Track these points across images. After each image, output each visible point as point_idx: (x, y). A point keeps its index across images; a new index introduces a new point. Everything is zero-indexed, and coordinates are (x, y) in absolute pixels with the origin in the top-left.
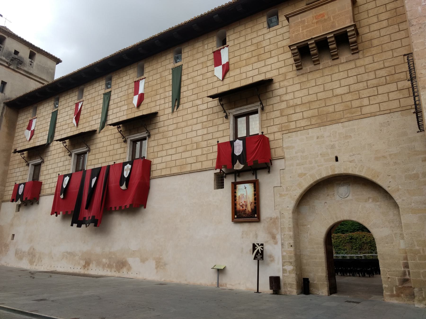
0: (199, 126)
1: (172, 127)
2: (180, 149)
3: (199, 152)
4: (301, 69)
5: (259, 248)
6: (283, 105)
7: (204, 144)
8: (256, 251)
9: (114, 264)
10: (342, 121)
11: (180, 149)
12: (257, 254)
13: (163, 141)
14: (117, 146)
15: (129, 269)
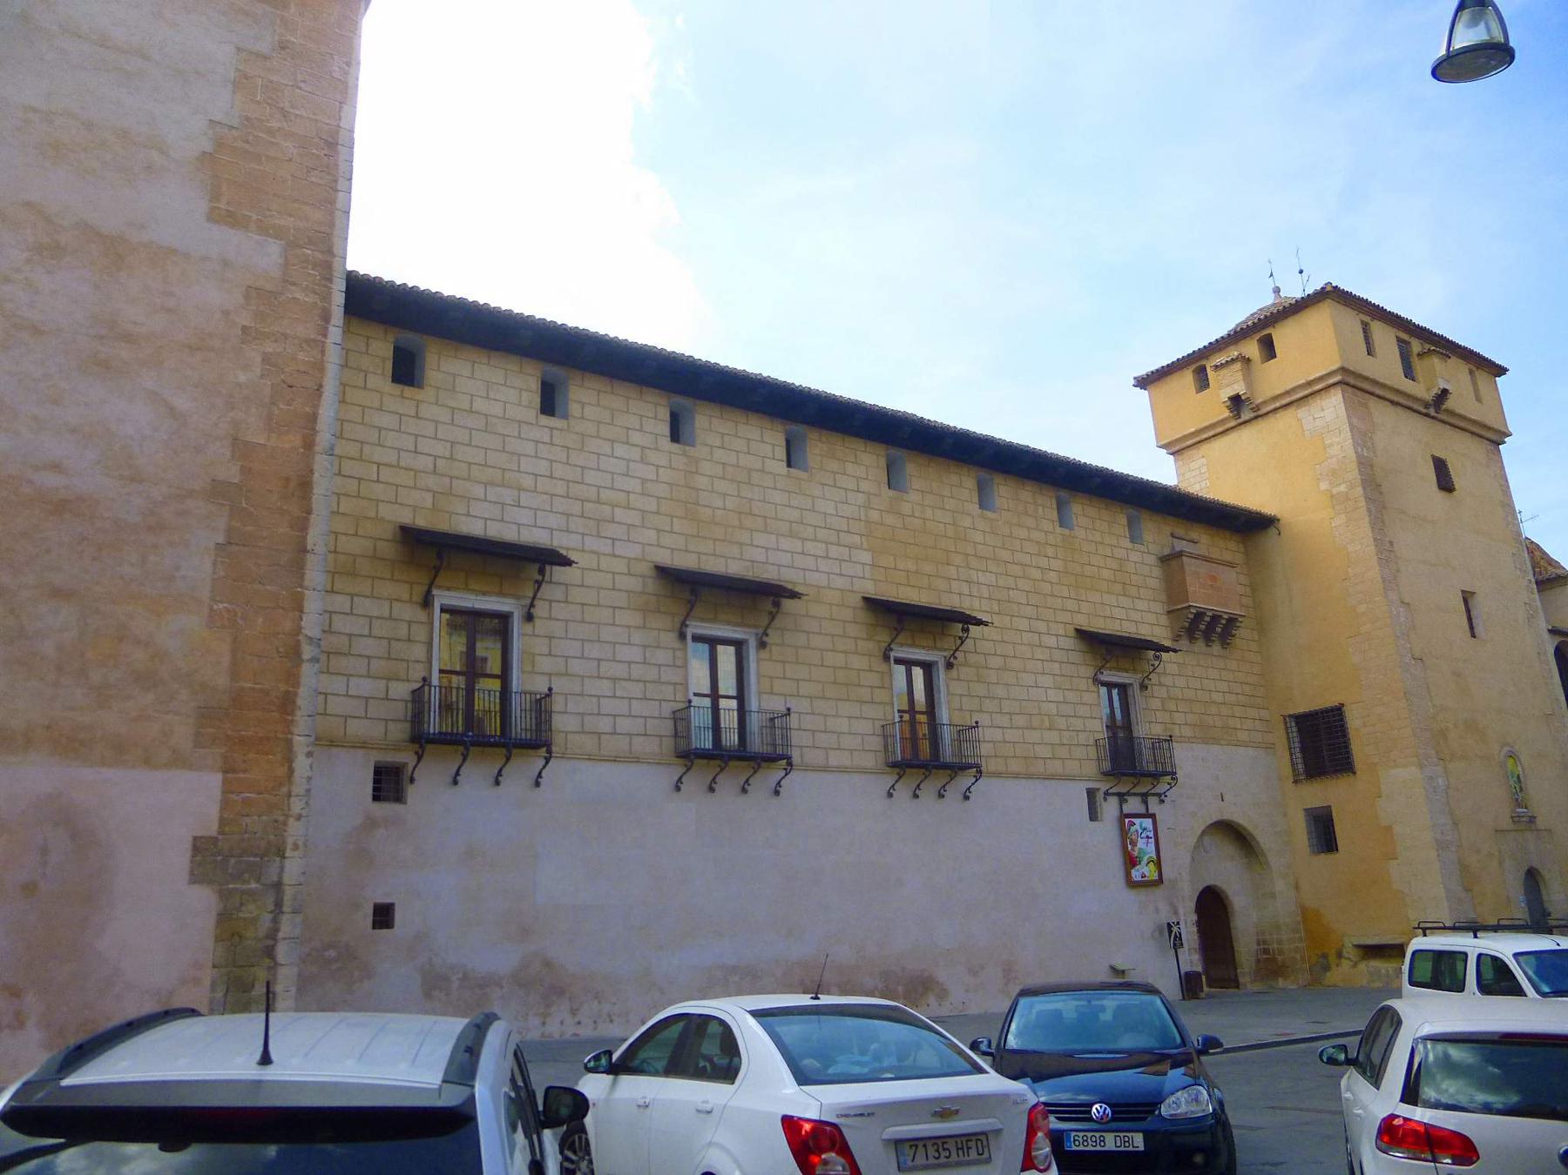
0: (1046, 681)
1: (995, 662)
2: (1020, 721)
3: (1053, 737)
4: (1177, 641)
5: (1175, 929)
6: (1163, 692)
7: (1061, 723)
8: (1173, 934)
9: (900, 988)
10: (1223, 742)
11: (1020, 721)
12: (1175, 940)
13: (980, 689)
14: (858, 662)
15: (943, 994)
